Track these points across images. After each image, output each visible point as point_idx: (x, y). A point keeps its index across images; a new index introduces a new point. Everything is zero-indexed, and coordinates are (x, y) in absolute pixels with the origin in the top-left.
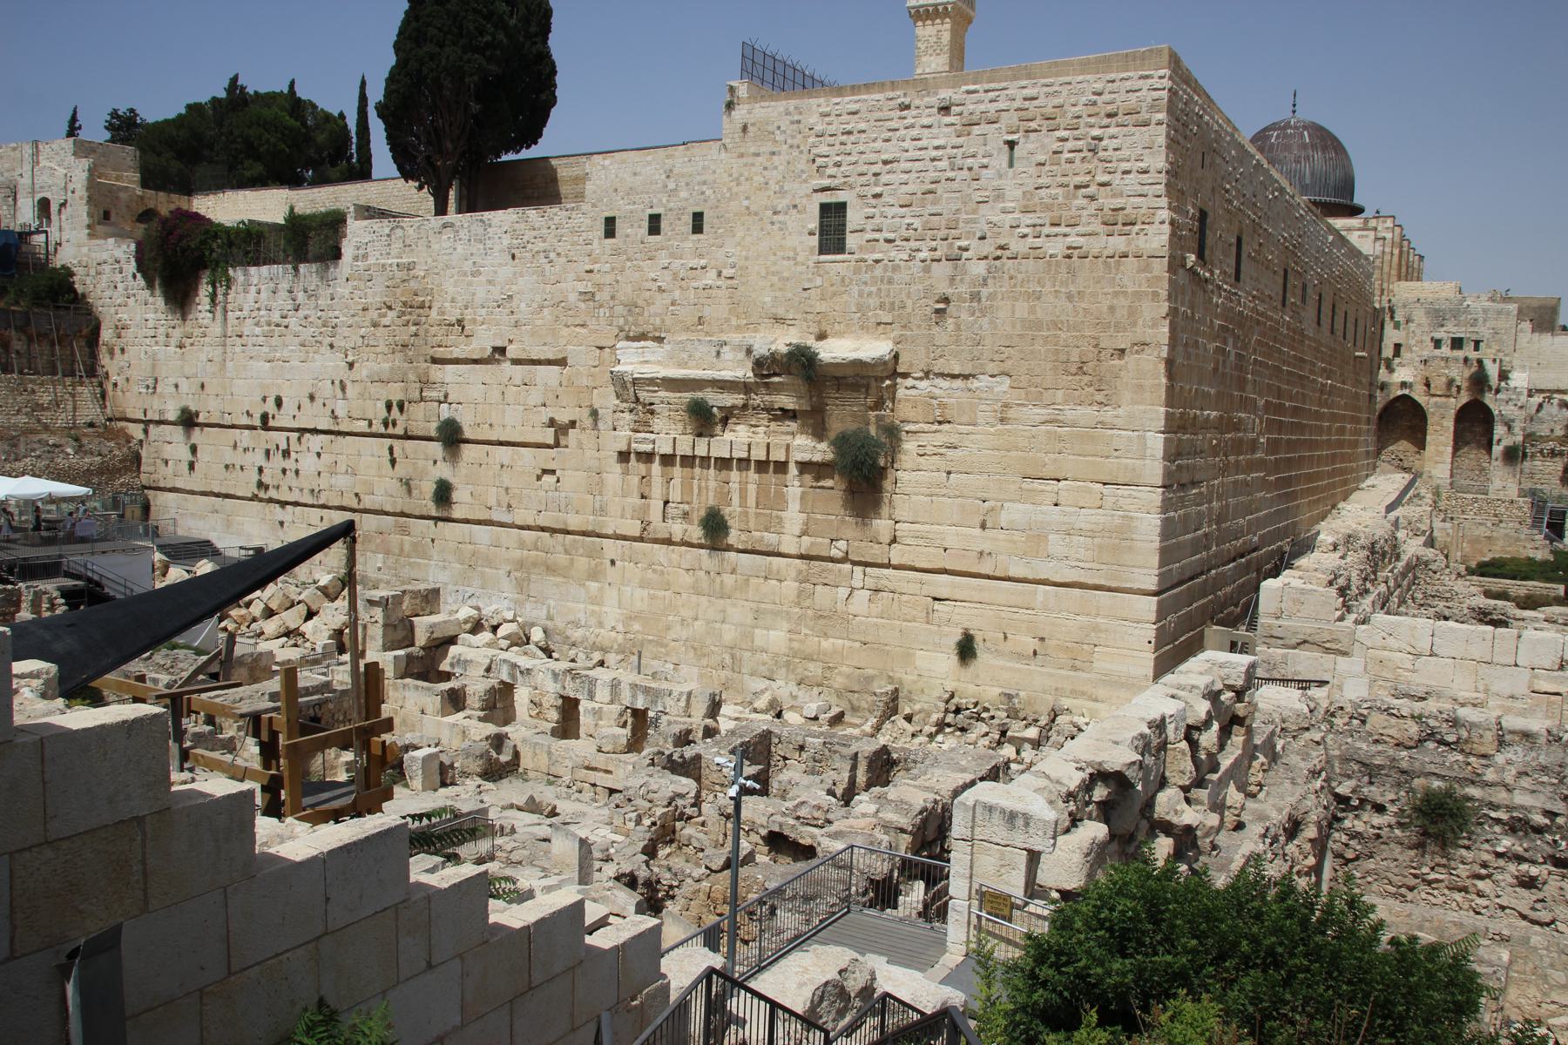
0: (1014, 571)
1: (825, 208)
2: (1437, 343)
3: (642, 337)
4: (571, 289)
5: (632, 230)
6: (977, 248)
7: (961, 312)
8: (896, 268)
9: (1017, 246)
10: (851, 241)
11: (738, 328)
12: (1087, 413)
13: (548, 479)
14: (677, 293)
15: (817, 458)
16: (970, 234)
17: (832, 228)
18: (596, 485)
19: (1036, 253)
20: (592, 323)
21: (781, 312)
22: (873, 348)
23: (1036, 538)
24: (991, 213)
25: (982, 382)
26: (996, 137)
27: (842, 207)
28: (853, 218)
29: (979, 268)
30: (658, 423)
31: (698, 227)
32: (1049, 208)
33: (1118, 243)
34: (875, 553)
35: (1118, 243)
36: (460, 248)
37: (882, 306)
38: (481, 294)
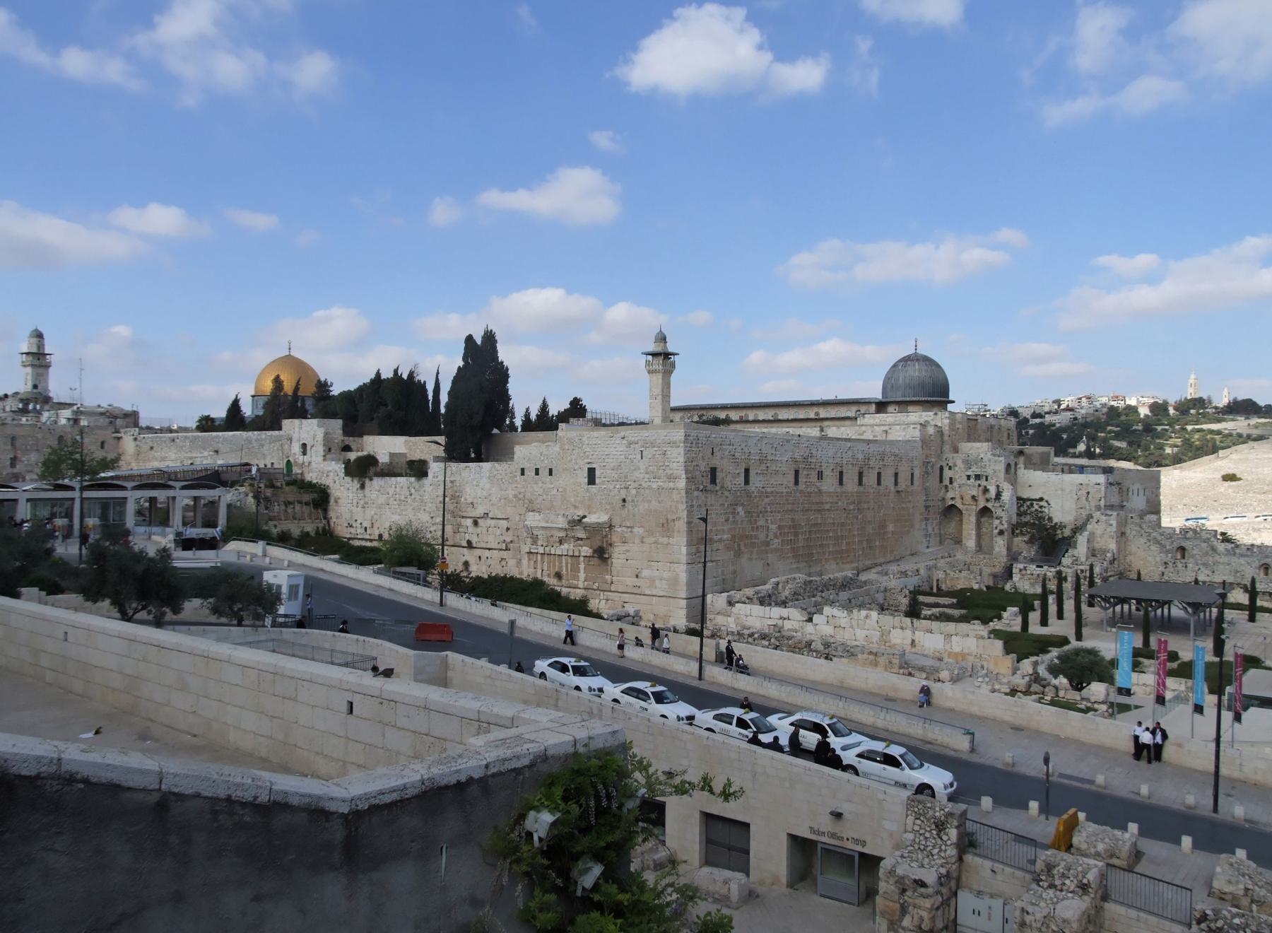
0: (647, 592)
2: (969, 477)
4: (511, 493)
5: (530, 473)
6: (633, 485)
7: (629, 505)
9: (645, 485)
12: (665, 540)
13: (503, 563)
17: (591, 479)
18: (519, 562)
19: (650, 488)
22: (603, 518)
23: (652, 580)
24: (637, 474)
25: (636, 530)
26: (638, 448)
28: (598, 473)
29: (634, 492)
30: (540, 543)
31: (551, 474)
33: (671, 485)
34: (606, 587)
35: (671, 485)
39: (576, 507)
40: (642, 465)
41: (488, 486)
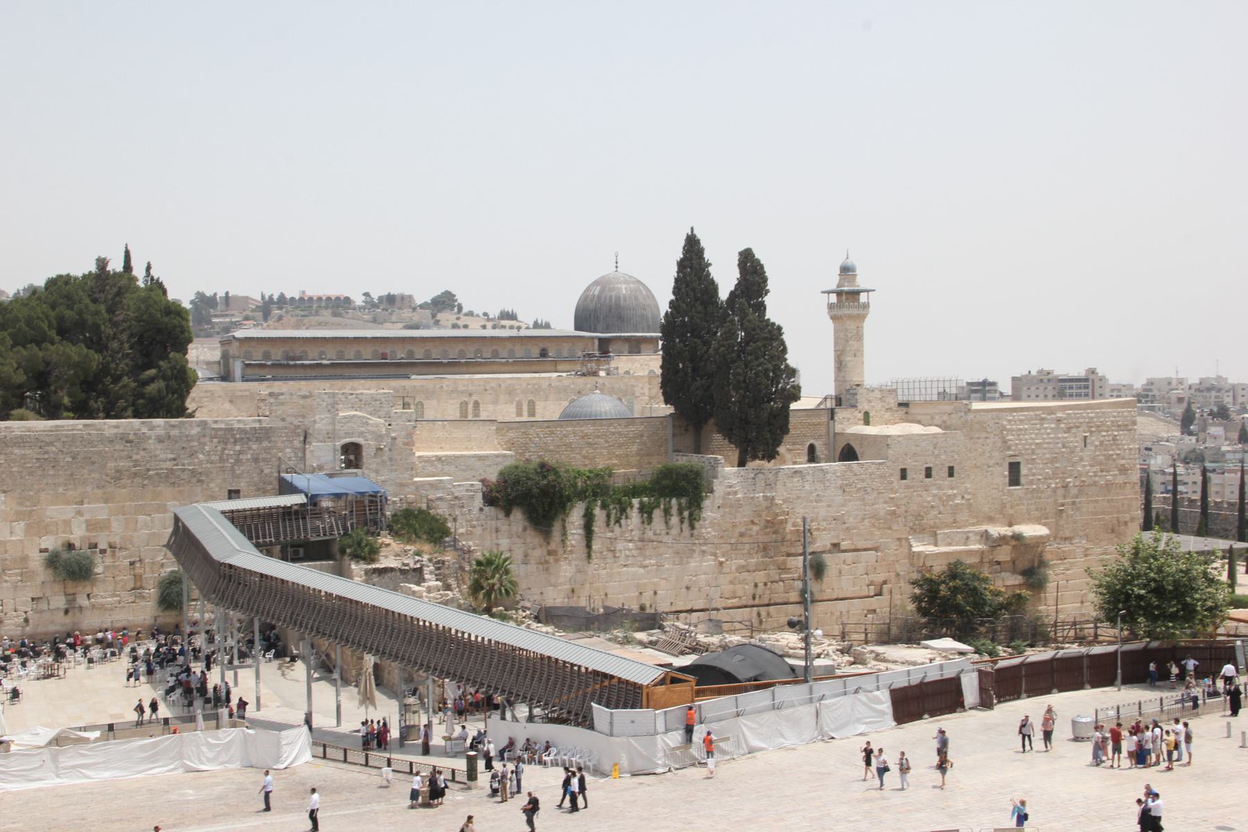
1: (1011, 464)
3: (923, 530)
5: (916, 476)
8: (1042, 492)
10: (1023, 480)
11: (973, 524)
14: (942, 508)
15: (1017, 582)
16: (1070, 476)
19: (1095, 484)
20: (895, 527)
21: (992, 514)
27: (1019, 463)
28: (1024, 470)
32: (1100, 464)
36: (807, 487)
37: (1037, 509)
38: (823, 513)
39: (991, 520)
40: (1087, 454)
41: (839, 499)
